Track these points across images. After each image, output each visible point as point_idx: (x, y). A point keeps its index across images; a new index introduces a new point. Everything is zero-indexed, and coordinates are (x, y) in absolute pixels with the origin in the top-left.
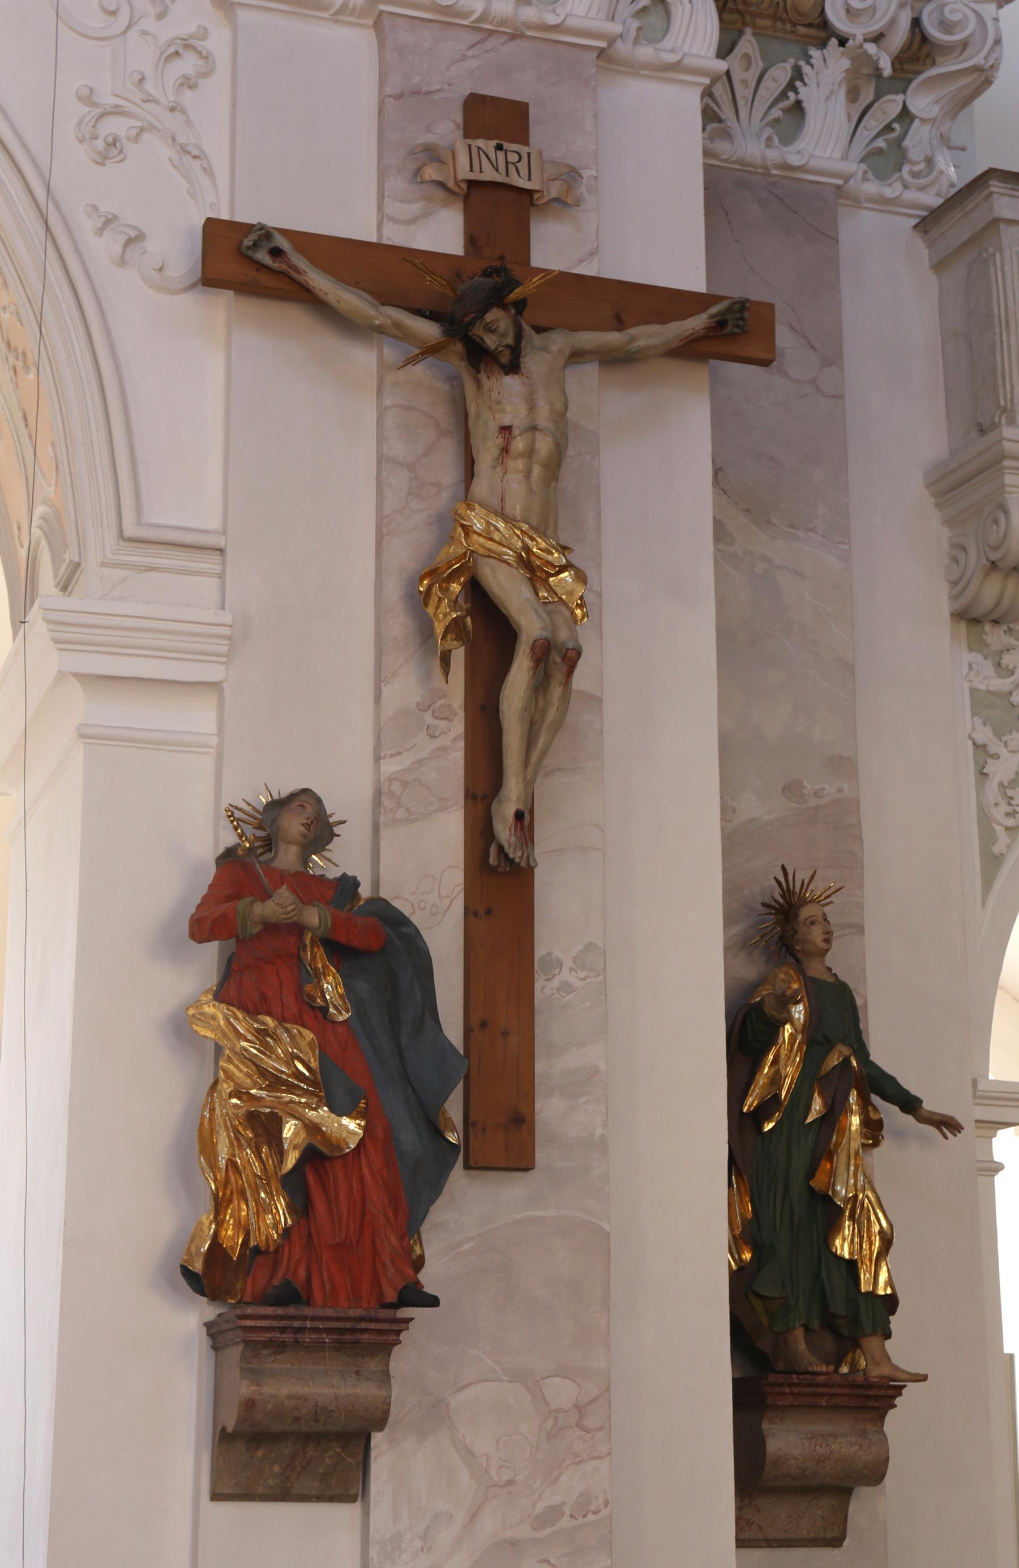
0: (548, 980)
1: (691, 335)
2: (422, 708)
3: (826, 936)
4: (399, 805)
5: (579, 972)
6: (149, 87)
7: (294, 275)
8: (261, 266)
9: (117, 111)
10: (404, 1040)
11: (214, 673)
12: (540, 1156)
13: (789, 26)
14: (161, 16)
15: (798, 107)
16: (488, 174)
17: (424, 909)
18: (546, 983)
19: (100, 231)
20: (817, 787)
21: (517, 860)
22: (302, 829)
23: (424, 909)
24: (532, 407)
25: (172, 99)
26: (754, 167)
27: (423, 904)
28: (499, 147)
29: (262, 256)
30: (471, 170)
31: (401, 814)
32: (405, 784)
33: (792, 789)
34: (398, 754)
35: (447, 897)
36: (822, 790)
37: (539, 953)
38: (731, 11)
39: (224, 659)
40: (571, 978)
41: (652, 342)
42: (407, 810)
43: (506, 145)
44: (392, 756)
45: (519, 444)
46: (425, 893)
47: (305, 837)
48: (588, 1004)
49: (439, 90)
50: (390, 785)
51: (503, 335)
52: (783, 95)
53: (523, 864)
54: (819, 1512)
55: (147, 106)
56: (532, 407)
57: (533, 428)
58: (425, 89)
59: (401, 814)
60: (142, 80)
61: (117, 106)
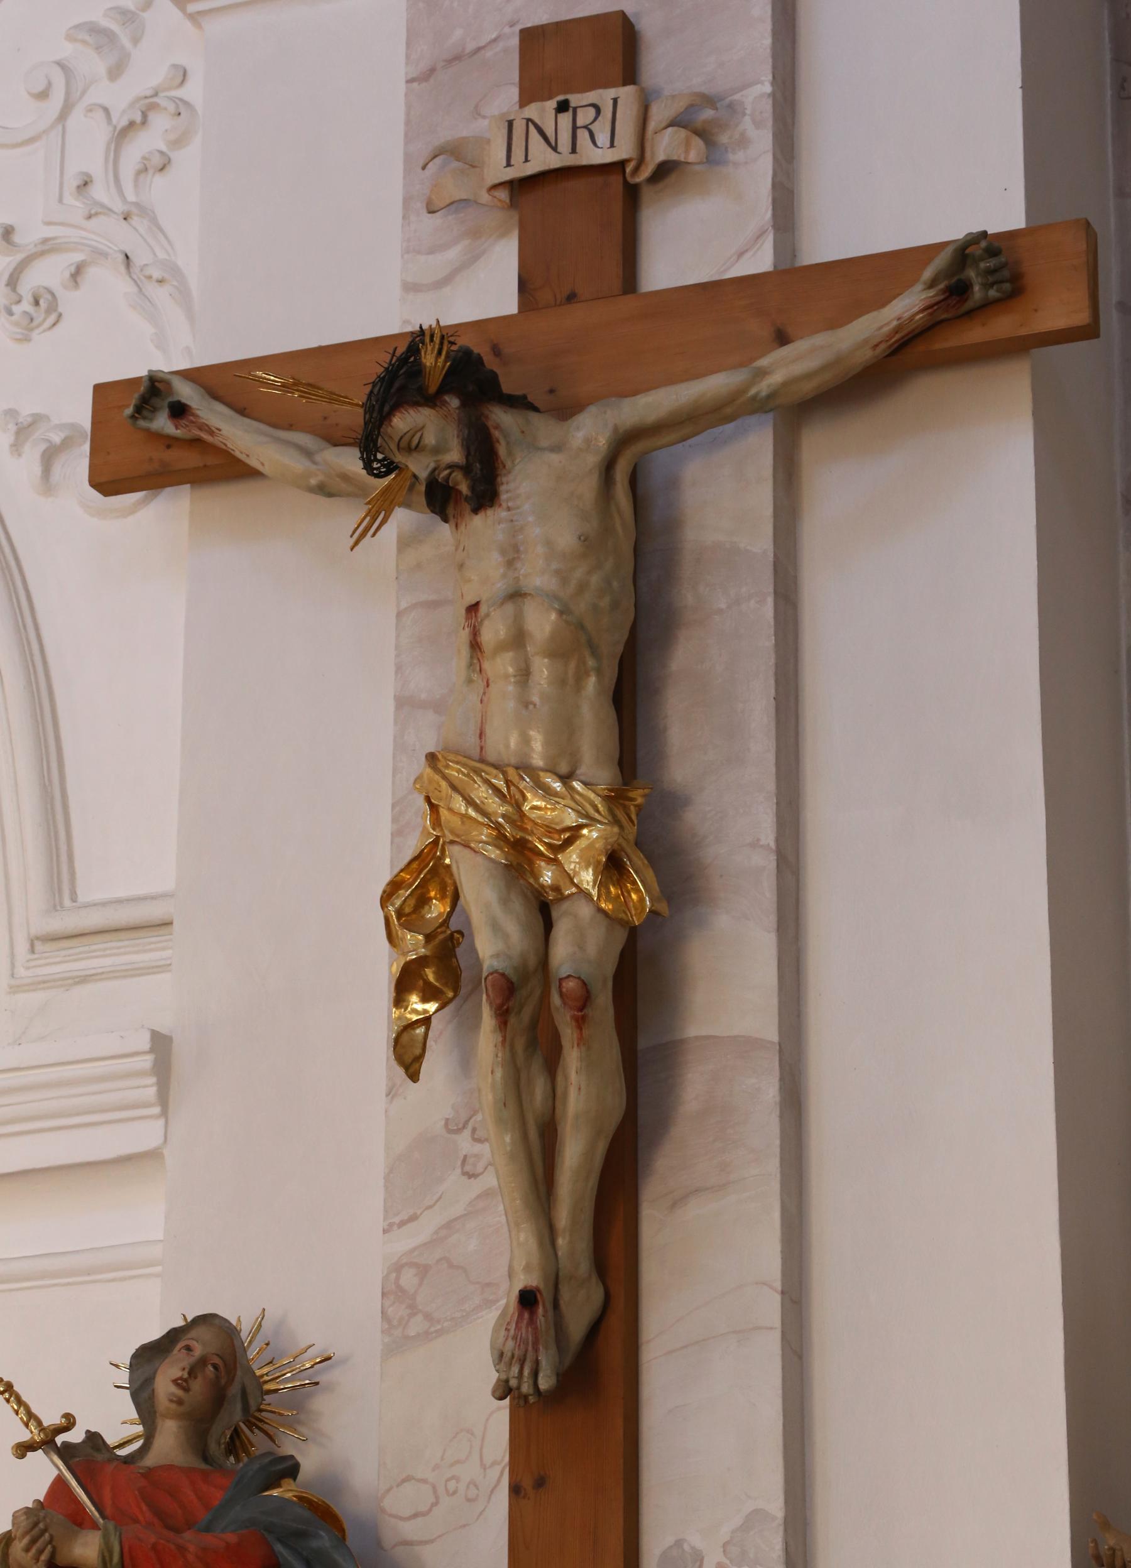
1: (896, 330)
2: (453, 1128)
6: (100, 192)
7: (205, 436)
8: (170, 442)
9: (48, 248)
11: (145, 1135)
14: (115, 72)
16: (542, 159)
17: (455, 1492)
19: (16, 447)
22: (173, 1389)
23: (455, 1492)
25: (131, 197)
27: (452, 1485)
28: (563, 107)
29: (162, 423)
30: (509, 165)
31: (417, 1325)
32: (423, 1271)
34: (413, 1218)
35: (494, 1463)
41: (799, 369)
42: (428, 1317)
43: (575, 99)
44: (402, 1224)
45: (494, 630)
46: (458, 1462)
47: (180, 1402)
49: (495, 40)
50: (398, 1278)
51: (437, 450)
55: (94, 222)
56: (512, 555)
57: (516, 595)
58: (471, 46)
59: (417, 1325)
61: (45, 241)
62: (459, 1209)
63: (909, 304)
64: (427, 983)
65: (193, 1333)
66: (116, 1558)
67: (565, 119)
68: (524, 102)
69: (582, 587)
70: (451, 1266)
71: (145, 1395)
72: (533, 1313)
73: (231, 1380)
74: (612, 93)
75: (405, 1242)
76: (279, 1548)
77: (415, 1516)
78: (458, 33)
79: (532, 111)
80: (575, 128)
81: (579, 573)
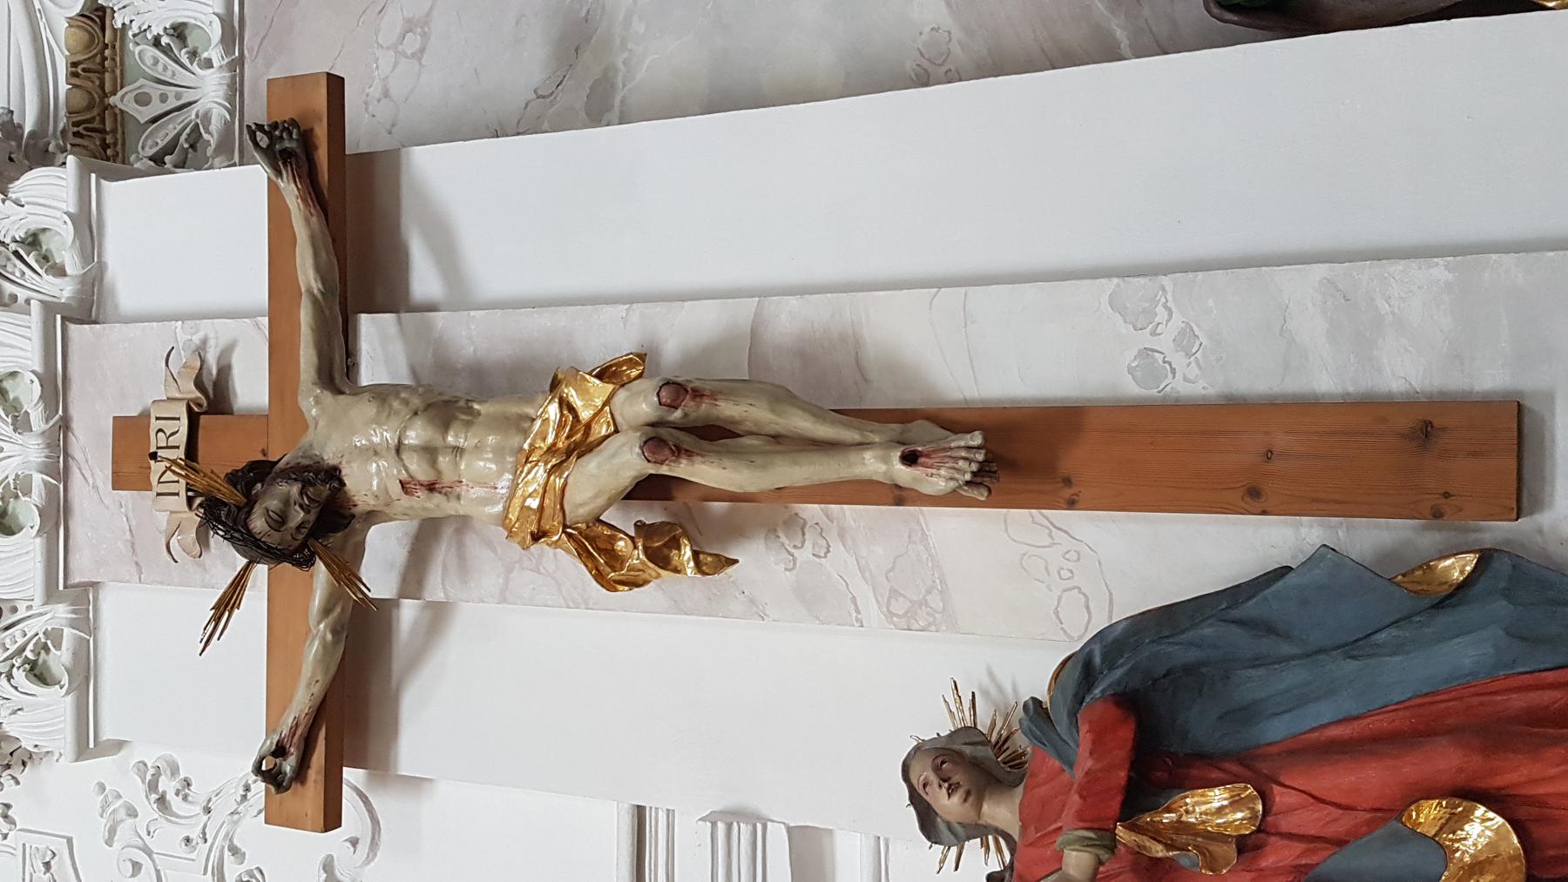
0: (1173, 371)
1: (304, 200)
4: (924, 603)
5: (1157, 320)
6: (195, 834)
10: (1286, 649)
12: (1489, 376)
13: (107, 52)
14: (132, 813)
15: (179, 32)
18: (1179, 375)
21: (974, 467)
24: (375, 452)
26: (233, 78)
28: (154, 456)
31: (935, 601)
32: (895, 593)
34: (854, 600)
35: (1050, 535)
37: (1132, 389)
38: (103, 121)
39: (759, 826)
40: (1169, 332)
42: (929, 592)
43: (153, 449)
44: (858, 612)
48: (1211, 303)
50: (897, 616)
52: (167, 51)
53: (980, 457)
56: (375, 452)
57: (399, 449)
60: (188, 840)
62: (852, 561)
63: (290, 190)
64: (664, 545)
65: (914, 781)
66: (1091, 834)
67: (160, 452)
68: (149, 487)
69: (406, 402)
70: (892, 569)
71: (959, 829)
72: (921, 454)
73: (960, 754)
74: (153, 420)
75: (872, 611)
76: (1097, 692)
77: (1088, 607)
78: (120, 544)
79: (154, 479)
80: (167, 447)
81: (396, 404)
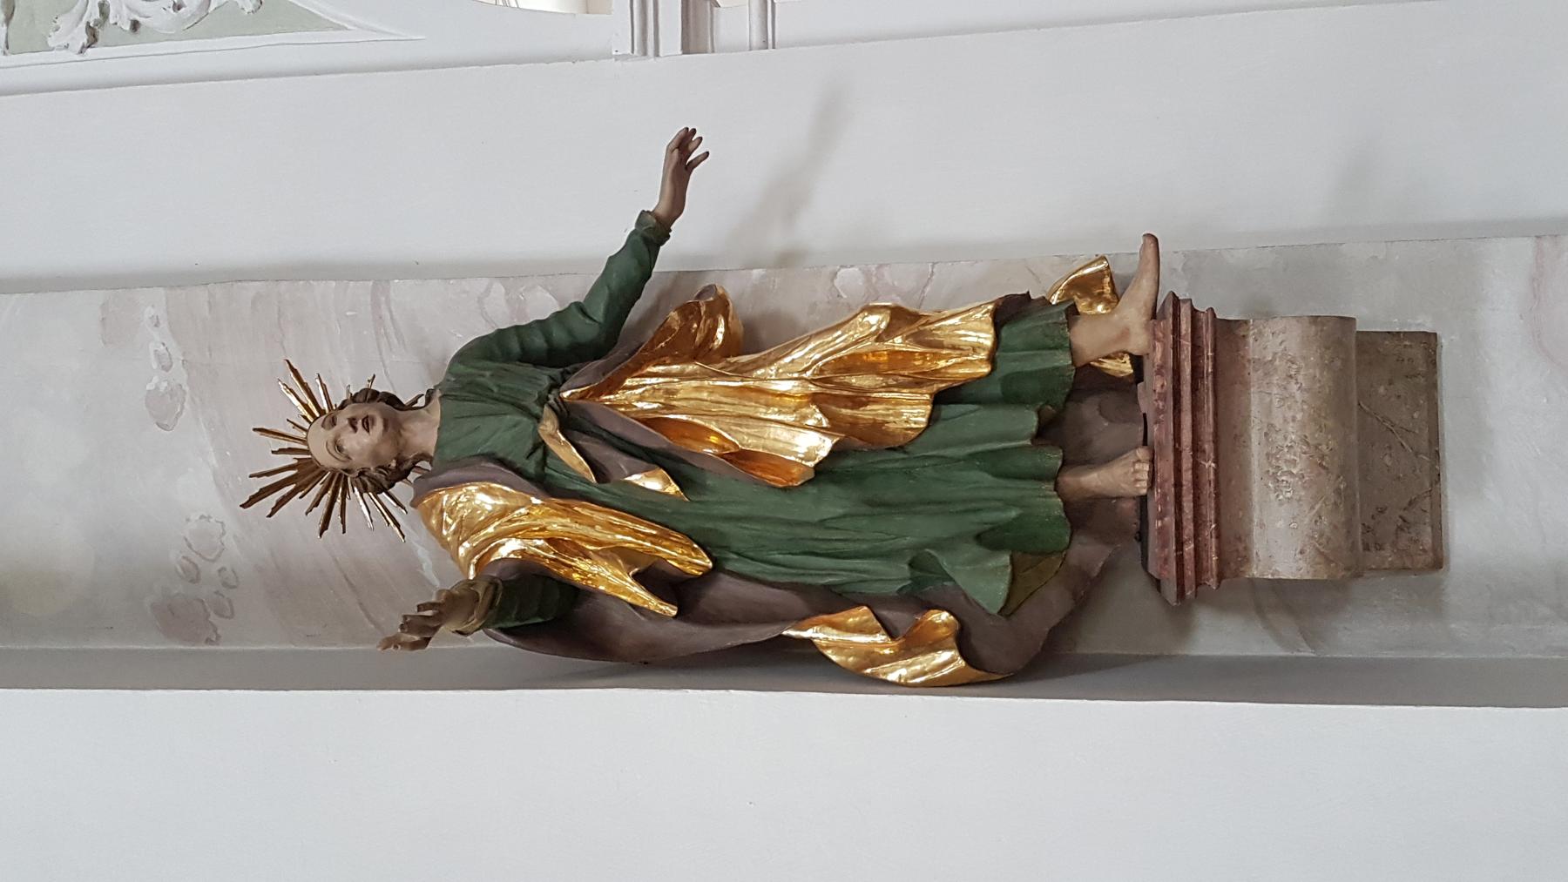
3: (359, 425)
20: (155, 366)
33: (163, 411)
36: (158, 356)
54: (1382, 390)
